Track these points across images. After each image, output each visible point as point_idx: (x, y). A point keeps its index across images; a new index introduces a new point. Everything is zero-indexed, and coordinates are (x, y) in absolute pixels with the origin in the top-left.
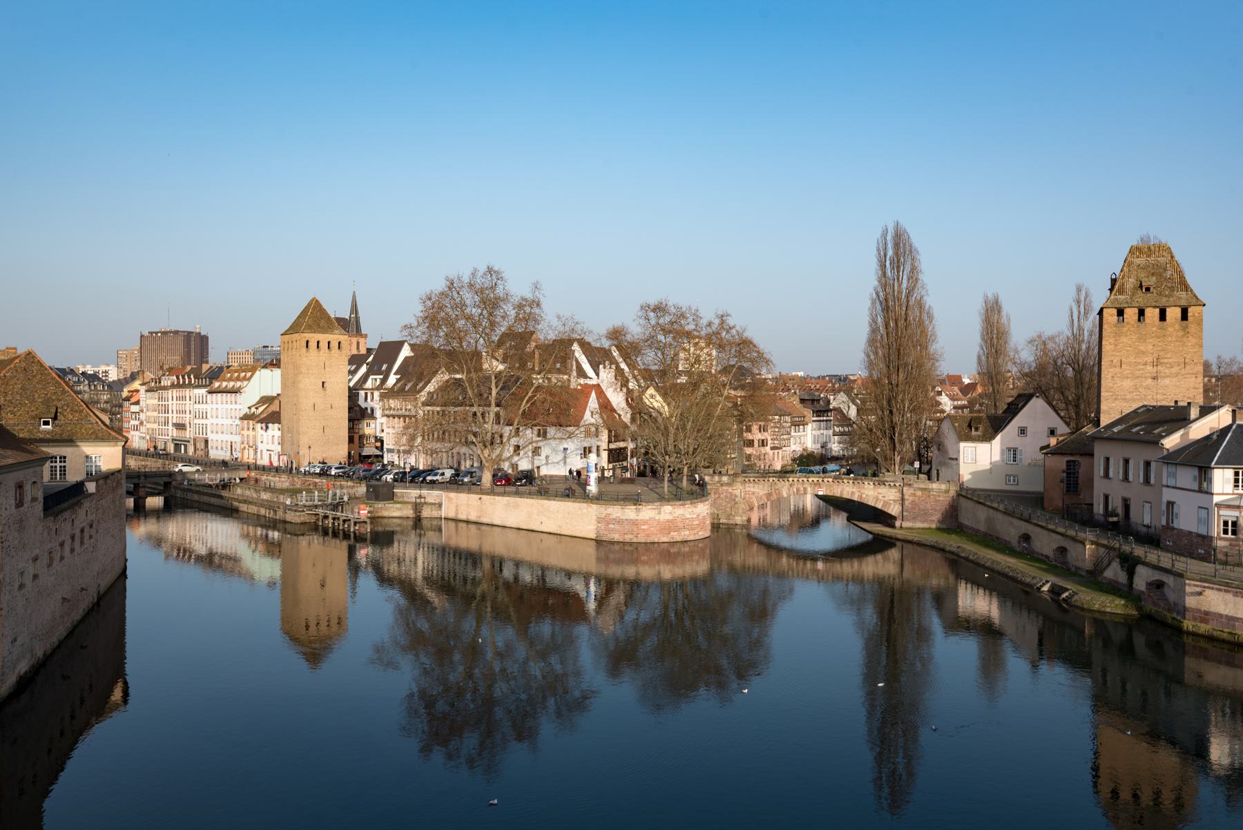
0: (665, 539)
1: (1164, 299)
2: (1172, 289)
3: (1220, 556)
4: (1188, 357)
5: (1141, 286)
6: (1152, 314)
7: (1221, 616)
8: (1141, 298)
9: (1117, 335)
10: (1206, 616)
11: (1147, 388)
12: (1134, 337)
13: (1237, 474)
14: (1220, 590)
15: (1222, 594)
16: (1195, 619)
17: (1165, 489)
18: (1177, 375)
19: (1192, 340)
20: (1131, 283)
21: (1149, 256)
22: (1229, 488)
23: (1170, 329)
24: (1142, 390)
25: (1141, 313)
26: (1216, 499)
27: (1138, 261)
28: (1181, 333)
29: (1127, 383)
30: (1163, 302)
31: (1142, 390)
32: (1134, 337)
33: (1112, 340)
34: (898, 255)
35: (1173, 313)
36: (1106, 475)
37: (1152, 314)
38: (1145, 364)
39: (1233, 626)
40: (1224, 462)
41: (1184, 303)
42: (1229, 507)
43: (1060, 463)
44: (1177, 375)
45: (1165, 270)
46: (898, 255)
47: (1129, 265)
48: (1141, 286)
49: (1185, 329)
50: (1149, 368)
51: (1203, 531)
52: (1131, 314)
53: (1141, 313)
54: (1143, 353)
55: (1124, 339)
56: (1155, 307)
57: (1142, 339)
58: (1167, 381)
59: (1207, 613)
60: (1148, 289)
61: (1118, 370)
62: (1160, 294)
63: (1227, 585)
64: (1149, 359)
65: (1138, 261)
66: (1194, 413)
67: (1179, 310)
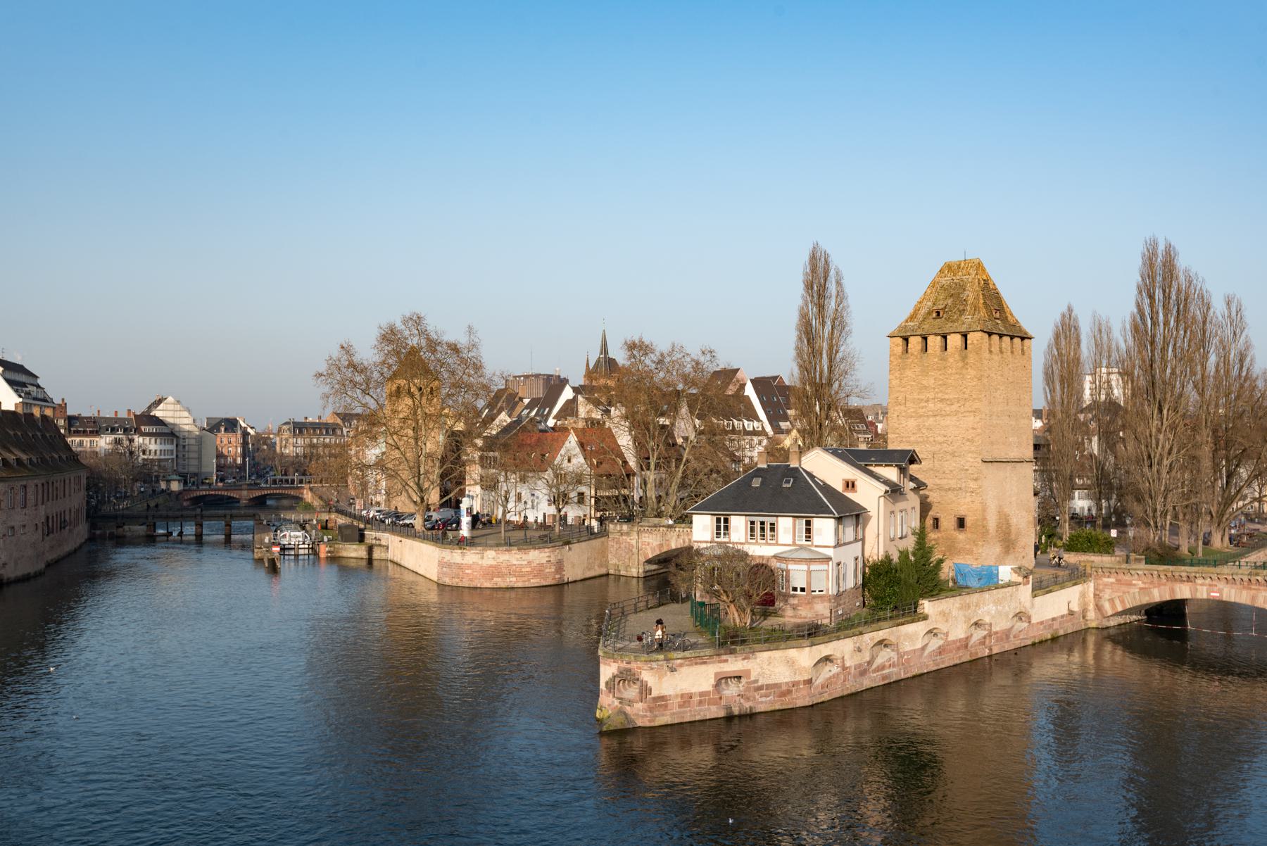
0: (487, 585)
6: (935, 342)
12: (918, 369)
13: (718, 521)
19: (972, 372)
23: (951, 360)
28: (960, 364)
29: (912, 423)
33: (897, 374)
34: (819, 279)
35: (955, 340)
37: (935, 342)
38: (927, 401)
41: (963, 329)
44: (957, 412)
46: (819, 279)
49: (964, 358)
52: (915, 342)
54: (926, 388)
55: (909, 373)
56: (936, 334)
57: (925, 372)
58: (948, 421)
60: (938, 313)
65: (943, 281)
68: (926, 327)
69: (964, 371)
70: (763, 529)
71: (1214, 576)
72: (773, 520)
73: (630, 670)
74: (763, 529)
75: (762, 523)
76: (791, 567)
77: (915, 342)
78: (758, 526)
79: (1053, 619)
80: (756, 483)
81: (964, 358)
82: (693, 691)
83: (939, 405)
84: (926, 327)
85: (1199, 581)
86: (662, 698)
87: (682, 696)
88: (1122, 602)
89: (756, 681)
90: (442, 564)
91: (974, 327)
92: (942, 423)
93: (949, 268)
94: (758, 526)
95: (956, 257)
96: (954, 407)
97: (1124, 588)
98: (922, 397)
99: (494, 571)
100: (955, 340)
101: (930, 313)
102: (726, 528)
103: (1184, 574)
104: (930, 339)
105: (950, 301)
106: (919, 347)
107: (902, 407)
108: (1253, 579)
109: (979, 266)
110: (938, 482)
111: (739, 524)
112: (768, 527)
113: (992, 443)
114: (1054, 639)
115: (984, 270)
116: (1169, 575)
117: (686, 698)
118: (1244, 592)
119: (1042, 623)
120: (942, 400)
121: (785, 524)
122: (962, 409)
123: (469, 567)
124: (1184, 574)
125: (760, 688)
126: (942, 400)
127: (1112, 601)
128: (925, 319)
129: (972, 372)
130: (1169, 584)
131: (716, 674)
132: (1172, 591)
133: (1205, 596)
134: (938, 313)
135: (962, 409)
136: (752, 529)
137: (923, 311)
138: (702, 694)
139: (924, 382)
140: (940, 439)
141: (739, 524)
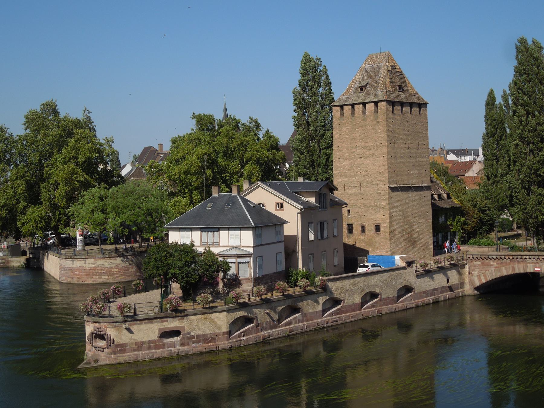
0: (90, 281)
11: (358, 167)
28: (374, 123)
29: (347, 163)
33: (337, 131)
41: (375, 100)
49: (376, 118)
54: (355, 139)
55: (344, 129)
56: (359, 104)
68: (355, 100)
76: (230, 260)
79: (434, 290)
82: (144, 340)
83: (363, 150)
84: (354, 98)
86: (122, 345)
87: (136, 344)
88: (485, 276)
89: (189, 333)
90: (62, 268)
96: (372, 151)
97: (486, 268)
98: (353, 145)
99: (93, 272)
100: (370, 107)
101: (357, 89)
106: (350, 112)
107: (341, 153)
109: (389, 57)
110: (363, 201)
113: (397, 175)
114: (436, 302)
115: (392, 59)
117: (139, 346)
119: (425, 292)
123: (77, 269)
125: (193, 337)
126: (364, 147)
127: (479, 276)
128: (354, 92)
131: (160, 329)
133: (532, 271)
134: (361, 89)
137: (353, 88)
138: (150, 342)
139: (354, 135)
140: (364, 173)
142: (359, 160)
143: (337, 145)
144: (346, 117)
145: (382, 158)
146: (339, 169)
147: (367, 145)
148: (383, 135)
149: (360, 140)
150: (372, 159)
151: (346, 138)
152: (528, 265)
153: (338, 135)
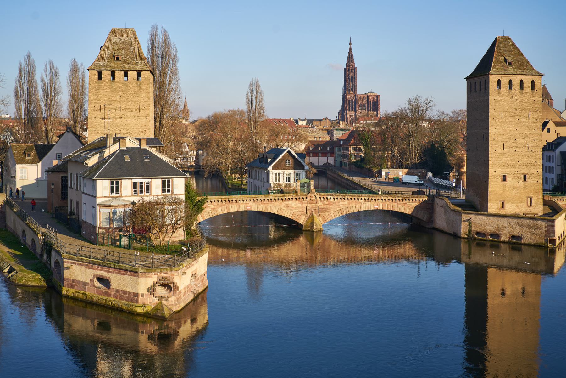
1: (127, 65)
2: (133, 59)
3: (101, 240)
4: (141, 105)
5: (114, 56)
6: (119, 75)
7: (79, 281)
8: (113, 64)
9: (98, 89)
10: (73, 283)
11: (117, 125)
12: (108, 90)
14: (78, 264)
15: (80, 267)
16: (68, 286)
17: (83, 195)
18: (135, 117)
20: (108, 53)
21: (121, 36)
22: (107, 192)
23: (131, 86)
24: (113, 127)
25: (113, 74)
26: (98, 201)
27: (115, 39)
28: (137, 89)
30: (127, 67)
31: (113, 127)
32: (108, 90)
33: (94, 92)
35: (132, 75)
36: (71, 187)
37: (119, 75)
38: (115, 109)
39: (85, 288)
40: (103, 176)
41: (138, 68)
42: (105, 206)
43: (58, 178)
44: (135, 117)
45: (130, 46)
47: (109, 42)
48: (114, 56)
49: (139, 85)
50: (118, 112)
51: (93, 224)
53: (113, 74)
55: (102, 92)
56: (121, 70)
57: (113, 92)
58: (129, 121)
59: (73, 281)
60: (118, 58)
61: (98, 113)
62: (125, 62)
63: (82, 261)
64: (118, 106)
65: (115, 39)
66: (110, 141)
67: (135, 73)
69: (139, 93)
70: (141, 187)
71: (248, 199)
72: (150, 180)
73: (166, 278)
74: (141, 187)
75: (141, 183)
77: (106, 74)
78: (138, 186)
80: (127, 158)
81: (139, 85)
83: (123, 112)
85: (242, 202)
91: (145, 68)
92: (126, 122)
93: (114, 32)
94: (138, 186)
95: (120, 26)
96: (134, 113)
100: (132, 75)
102: (117, 188)
103: (234, 200)
104: (117, 73)
105: (123, 51)
108: (266, 199)
111: (127, 184)
112: (144, 186)
116: (227, 200)
118: (262, 206)
120: (125, 109)
121: (156, 184)
122: (138, 114)
124: (234, 200)
126: (125, 109)
129: (144, 94)
130: (227, 205)
132: (228, 208)
135: (138, 114)
136: (135, 188)
139: (113, 98)
141: (127, 184)
142: (118, 120)
143: (93, 105)
144: (105, 81)
145: (145, 119)
146: (95, 127)
147: (128, 107)
148: (146, 100)
149: (120, 102)
150: (134, 119)
151: (104, 100)
152: (241, 205)
153: (95, 97)
